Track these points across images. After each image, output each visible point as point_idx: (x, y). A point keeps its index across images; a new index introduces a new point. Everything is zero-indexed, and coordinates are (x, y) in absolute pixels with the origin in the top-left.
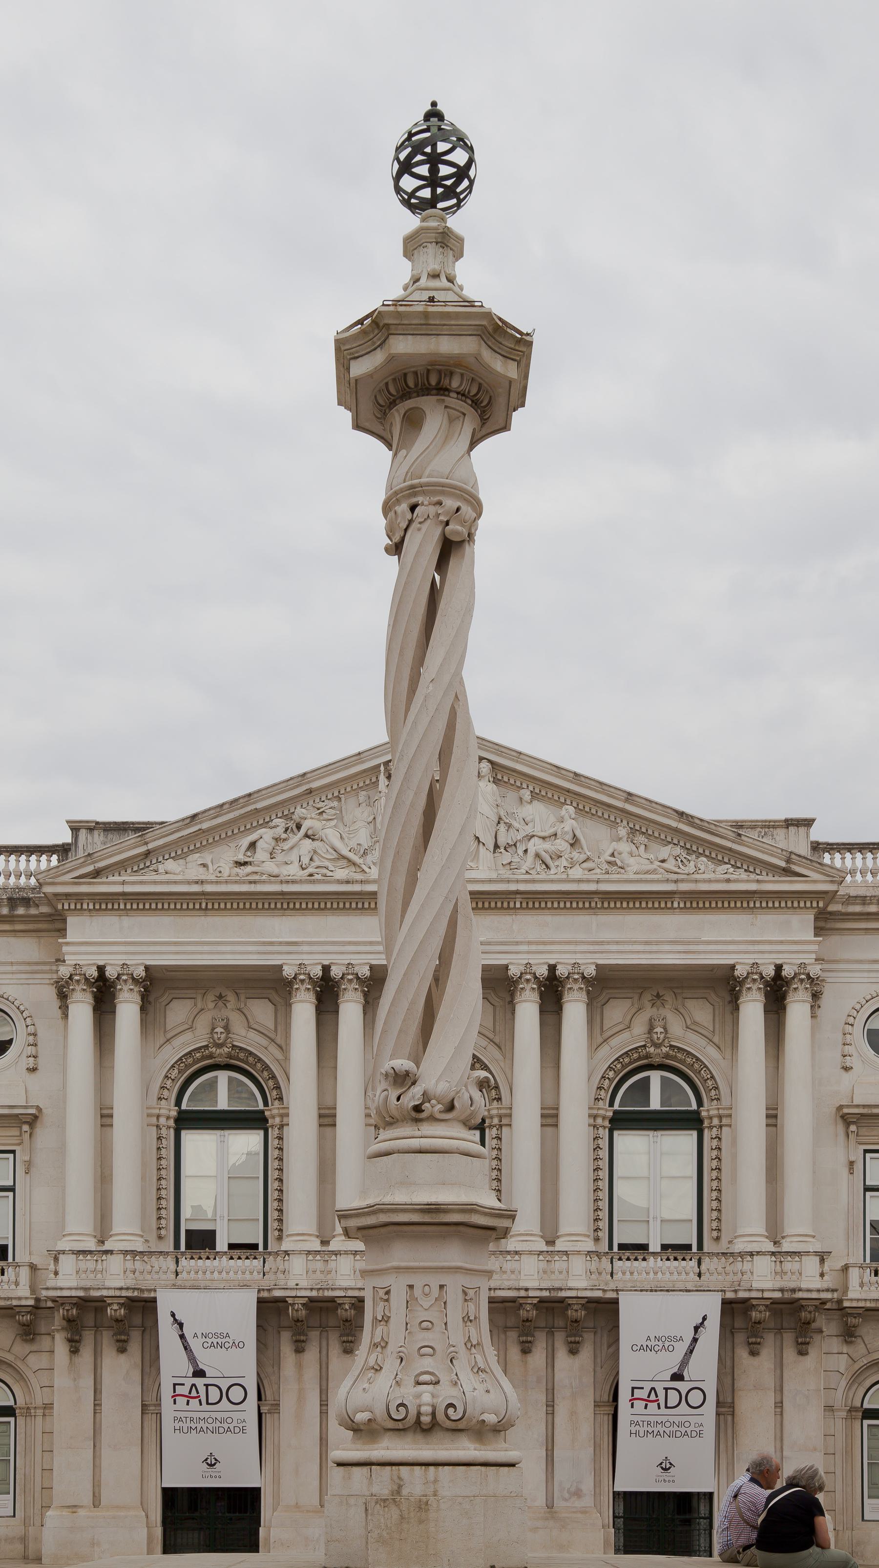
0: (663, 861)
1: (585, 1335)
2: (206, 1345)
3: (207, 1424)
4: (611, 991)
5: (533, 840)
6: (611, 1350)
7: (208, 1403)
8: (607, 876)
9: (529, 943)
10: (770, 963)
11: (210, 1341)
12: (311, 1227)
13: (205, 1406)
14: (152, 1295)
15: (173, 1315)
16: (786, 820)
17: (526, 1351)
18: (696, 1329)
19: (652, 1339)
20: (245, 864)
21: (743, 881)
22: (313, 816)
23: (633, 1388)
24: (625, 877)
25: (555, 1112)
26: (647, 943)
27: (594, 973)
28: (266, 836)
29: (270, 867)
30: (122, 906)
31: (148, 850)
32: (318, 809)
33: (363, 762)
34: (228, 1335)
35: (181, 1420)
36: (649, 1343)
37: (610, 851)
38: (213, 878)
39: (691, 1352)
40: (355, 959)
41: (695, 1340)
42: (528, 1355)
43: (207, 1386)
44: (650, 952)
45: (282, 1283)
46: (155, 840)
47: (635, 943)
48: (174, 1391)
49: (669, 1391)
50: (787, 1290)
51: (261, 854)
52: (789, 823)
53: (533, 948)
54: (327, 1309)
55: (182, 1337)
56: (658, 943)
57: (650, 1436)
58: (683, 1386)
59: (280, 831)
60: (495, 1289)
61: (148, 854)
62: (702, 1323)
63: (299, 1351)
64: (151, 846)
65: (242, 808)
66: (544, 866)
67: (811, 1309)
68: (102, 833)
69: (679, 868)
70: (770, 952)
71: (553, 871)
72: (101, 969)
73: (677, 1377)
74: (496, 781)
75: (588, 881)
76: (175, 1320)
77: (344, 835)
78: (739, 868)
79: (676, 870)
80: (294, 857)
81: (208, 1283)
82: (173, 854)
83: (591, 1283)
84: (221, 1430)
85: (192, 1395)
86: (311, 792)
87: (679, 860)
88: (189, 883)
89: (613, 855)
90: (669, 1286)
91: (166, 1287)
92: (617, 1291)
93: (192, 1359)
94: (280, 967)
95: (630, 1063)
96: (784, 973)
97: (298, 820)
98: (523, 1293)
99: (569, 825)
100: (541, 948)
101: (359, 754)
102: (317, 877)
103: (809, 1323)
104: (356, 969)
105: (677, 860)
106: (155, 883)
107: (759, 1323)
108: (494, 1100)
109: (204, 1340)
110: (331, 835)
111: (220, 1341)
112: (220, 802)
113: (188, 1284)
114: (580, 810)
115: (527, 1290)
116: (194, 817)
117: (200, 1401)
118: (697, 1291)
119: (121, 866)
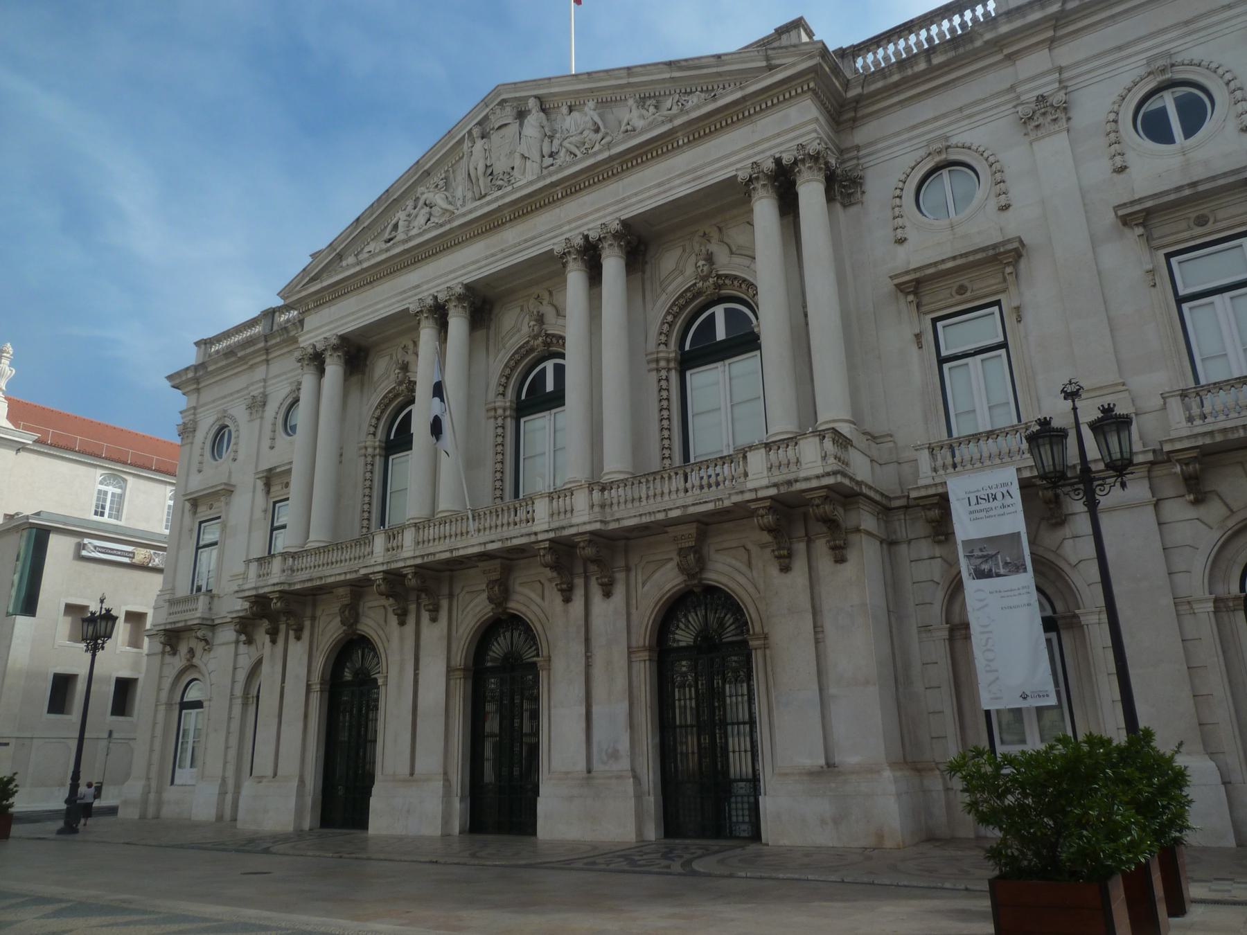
9: (569, 222)
16: (776, 30)
17: (567, 600)
26: (659, 185)
28: (401, 215)
31: (338, 254)
37: (625, 121)
42: (570, 604)
51: (401, 229)
52: (781, 31)
53: (573, 225)
60: (511, 538)
63: (402, 623)
64: (338, 251)
65: (386, 202)
67: (817, 501)
71: (579, 155)
74: (543, 110)
87: (680, 104)
96: (784, 162)
98: (533, 538)
100: (579, 223)
101: (449, 132)
110: (439, 199)
112: (371, 203)
115: (536, 534)
116: (358, 219)
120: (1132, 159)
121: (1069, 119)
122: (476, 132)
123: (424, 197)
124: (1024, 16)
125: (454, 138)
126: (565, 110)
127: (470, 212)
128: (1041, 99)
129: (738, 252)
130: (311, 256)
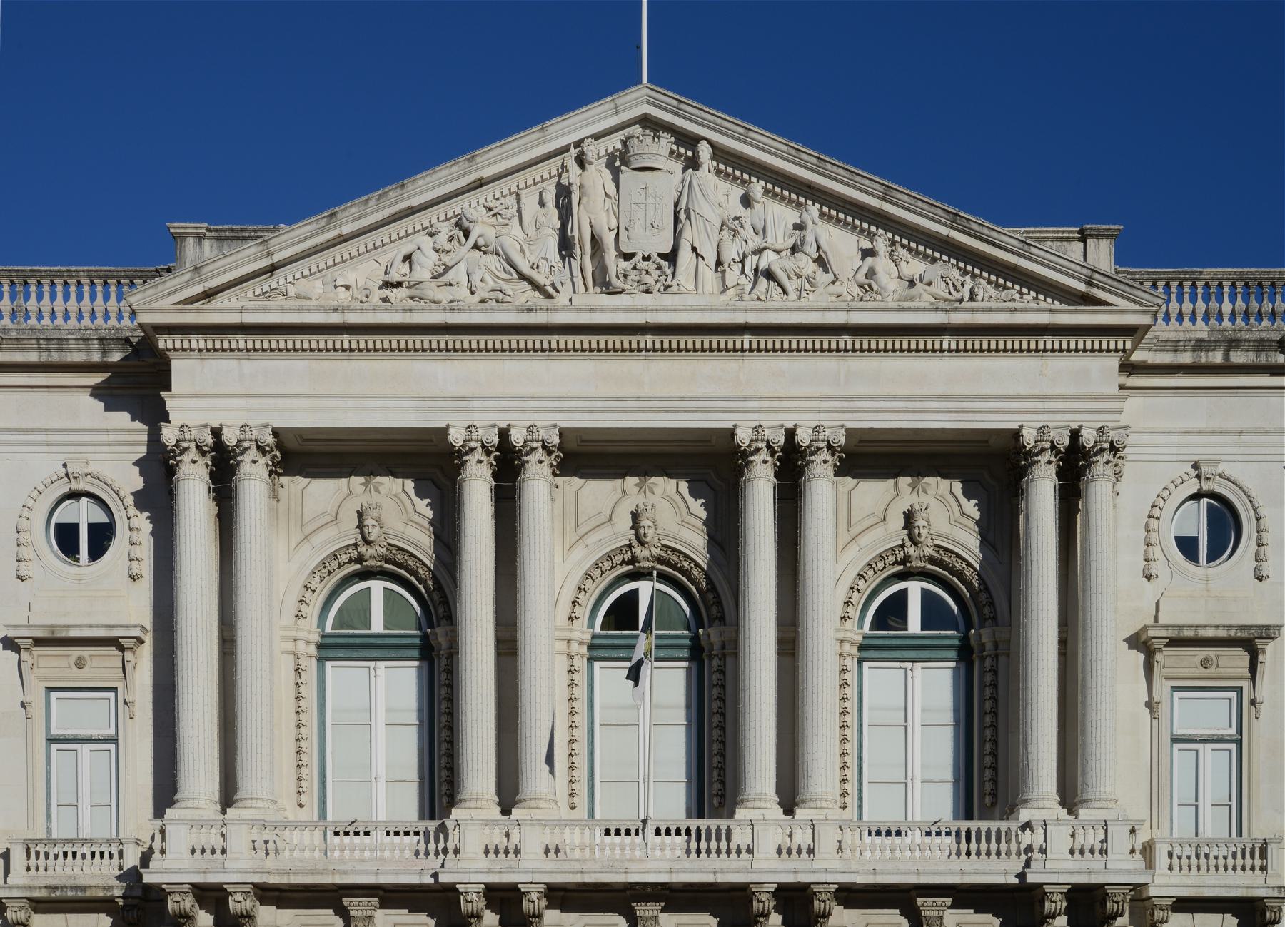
24: (882, 305)
33: (547, 141)
47: (895, 397)
66: (779, 290)
68: (215, 246)
69: (950, 293)
70: (1064, 412)
75: (836, 310)
77: (525, 247)
105: (947, 283)
127: (592, 310)
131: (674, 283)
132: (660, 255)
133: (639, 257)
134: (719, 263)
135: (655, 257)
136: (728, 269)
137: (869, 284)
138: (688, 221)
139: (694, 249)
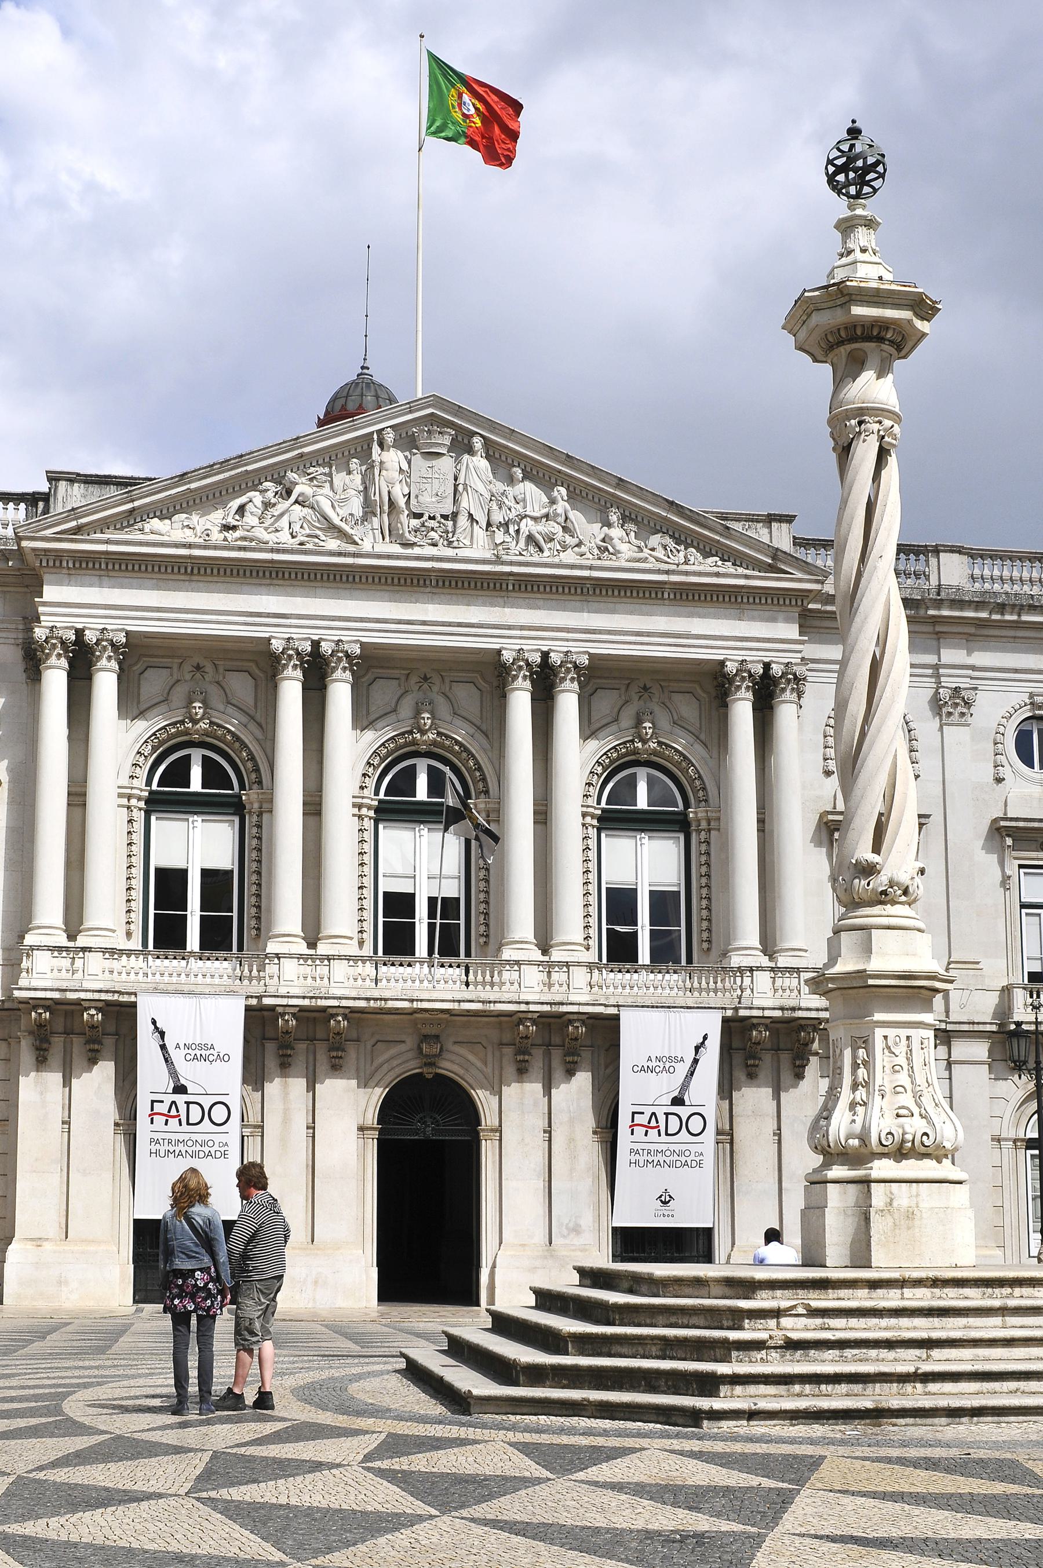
0: (653, 549)
1: (583, 1054)
2: (188, 1057)
3: (186, 1148)
4: (598, 681)
5: (524, 520)
6: (609, 1071)
7: (188, 1124)
8: (599, 562)
10: (758, 662)
11: (193, 1053)
12: (296, 927)
13: (185, 1127)
14: (133, 999)
15: (154, 1022)
18: (697, 1049)
19: (654, 1059)
20: (234, 528)
21: (732, 576)
22: (304, 481)
23: (153, 1102)
25: (544, 808)
27: (587, 662)
28: (257, 498)
29: (260, 533)
30: (103, 566)
32: (309, 474)
34: (212, 1047)
35: (157, 1142)
36: (650, 1064)
38: (198, 540)
39: (692, 1074)
40: (346, 636)
41: (696, 1061)
43: (188, 1103)
44: (642, 644)
45: (271, 990)
46: (141, 498)
48: (152, 1109)
49: (191, 1105)
50: (787, 1009)
54: (315, 1019)
55: (163, 1047)
56: (649, 634)
57: (171, 1156)
58: (683, 1111)
59: (270, 494)
61: (132, 511)
62: (703, 1043)
64: (137, 504)
69: (669, 557)
72: (80, 633)
73: (678, 1101)
74: (488, 457)
75: (581, 567)
76: (156, 1028)
78: (726, 561)
79: (666, 558)
80: (284, 522)
81: (192, 988)
82: (158, 514)
83: (593, 997)
84: (202, 1154)
85: (171, 1114)
86: (302, 456)
88: (176, 545)
89: (603, 540)
90: (670, 1002)
91: (146, 991)
92: (618, 1006)
93: (173, 1073)
94: (268, 640)
95: (618, 759)
97: (288, 485)
99: (562, 506)
102: (308, 546)
103: (807, 1045)
104: (346, 647)
106: (141, 544)
107: (759, 1043)
108: (481, 792)
109: (187, 1051)
111: (203, 1053)
113: (171, 988)
114: (571, 492)
117: (180, 1121)
118: (698, 1008)
119: (104, 525)
120: (1006, 772)
121: (972, 715)
122: (390, 437)
123: (297, 490)
124: (962, 610)
125: (356, 430)
126: (518, 473)
128: (957, 690)
129: (679, 723)
130: (54, 478)
131: (454, 539)
132: (442, 516)
133: (426, 517)
134: (489, 524)
135: (439, 518)
136: (496, 530)
137: (605, 548)
138: (465, 492)
139: (471, 515)
